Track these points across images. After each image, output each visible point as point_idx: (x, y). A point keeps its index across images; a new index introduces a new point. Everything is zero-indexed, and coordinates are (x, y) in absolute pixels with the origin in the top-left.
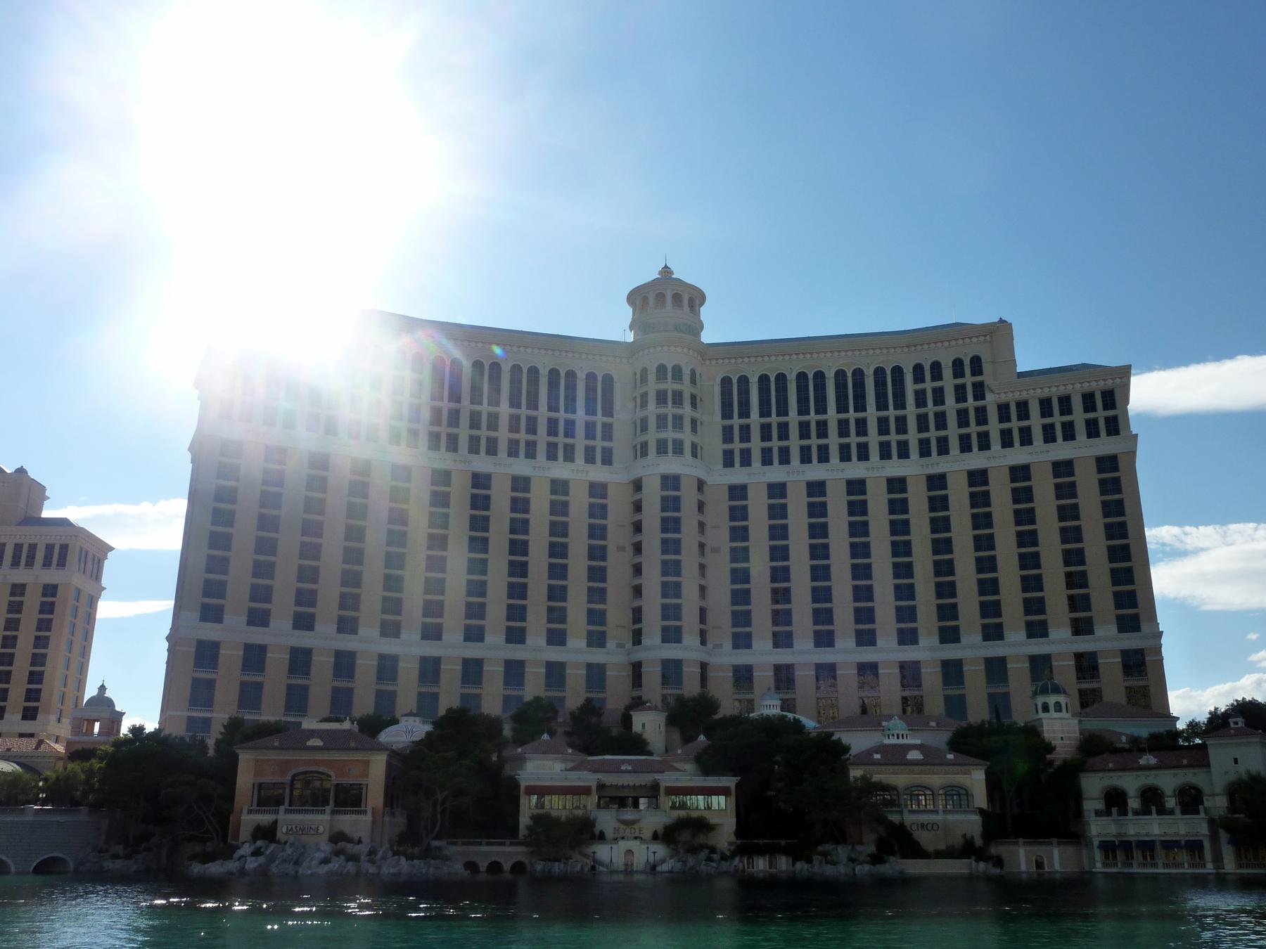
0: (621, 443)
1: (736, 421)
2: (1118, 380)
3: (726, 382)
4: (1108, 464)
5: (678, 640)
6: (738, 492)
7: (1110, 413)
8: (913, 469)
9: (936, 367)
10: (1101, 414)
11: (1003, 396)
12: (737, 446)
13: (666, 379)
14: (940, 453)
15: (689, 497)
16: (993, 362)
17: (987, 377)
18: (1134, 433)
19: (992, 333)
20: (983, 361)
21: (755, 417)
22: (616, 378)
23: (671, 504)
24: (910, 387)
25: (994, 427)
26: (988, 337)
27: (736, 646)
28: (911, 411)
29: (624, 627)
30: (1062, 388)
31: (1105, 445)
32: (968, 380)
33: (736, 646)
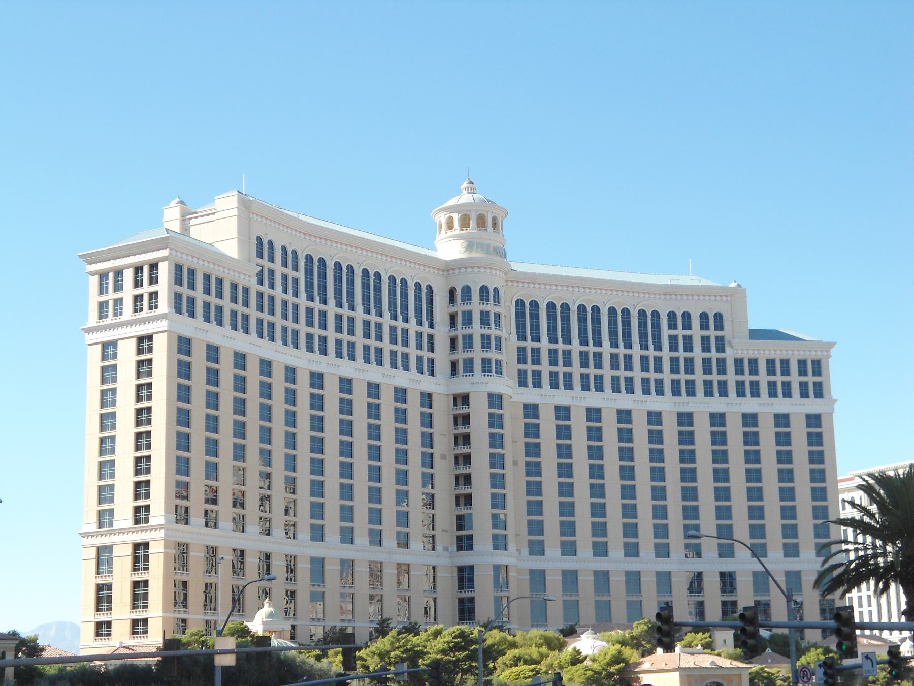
0: (442, 356)
2: (825, 353)
3: (520, 304)
4: (814, 420)
6: (531, 410)
7: (817, 379)
8: (667, 405)
9: (687, 316)
10: (810, 379)
11: (740, 352)
12: (529, 367)
13: (488, 300)
14: (688, 395)
16: (732, 321)
17: (726, 333)
18: (834, 398)
19: (732, 295)
20: (724, 318)
23: (496, 421)
24: (666, 332)
26: (729, 299)
27: (531, 553)
28: (666, 354)
29: (447, 531)
30: (784, 352)
31: (812, 406)
32: (712, 333)
33: (531, 553)
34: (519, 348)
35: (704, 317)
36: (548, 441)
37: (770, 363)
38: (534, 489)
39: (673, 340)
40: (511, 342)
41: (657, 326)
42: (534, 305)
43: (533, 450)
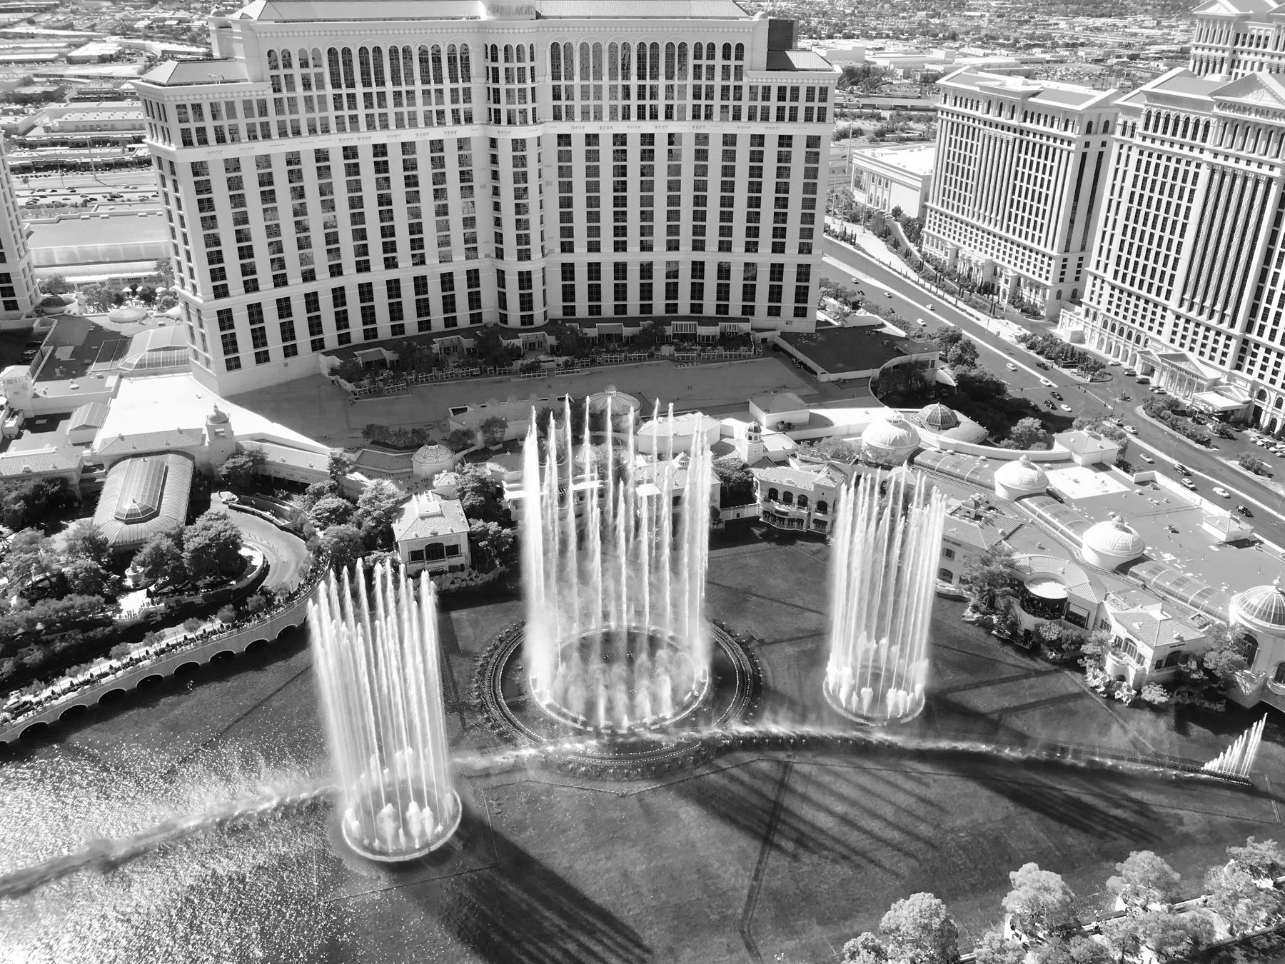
0: (479, 105)
1: (563, 83)
3: (555, 46)
5: (529, 258)
8: (686, 128)
9: (711, 47)
12: (563, 103)
15: (531, 153)
17: (745, 62)
21: (577, 81)
22: (470, 47)
23: (520, 161)
24: (691, 62)
25: (745, 104)
27: (563, 250)
28: (690, 81)
32: (733, 63)
33: (563, 250)
34: (554, 87)
35: (727, 47)
36: (579, 164)
37: (782, 90)
38: (566, 202)
39: (697, 68)
40: (545, 83)
41: (683, 54)
42: (568, 47)
43: (564, 172)
